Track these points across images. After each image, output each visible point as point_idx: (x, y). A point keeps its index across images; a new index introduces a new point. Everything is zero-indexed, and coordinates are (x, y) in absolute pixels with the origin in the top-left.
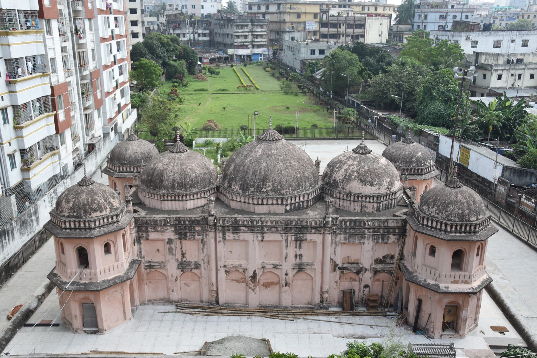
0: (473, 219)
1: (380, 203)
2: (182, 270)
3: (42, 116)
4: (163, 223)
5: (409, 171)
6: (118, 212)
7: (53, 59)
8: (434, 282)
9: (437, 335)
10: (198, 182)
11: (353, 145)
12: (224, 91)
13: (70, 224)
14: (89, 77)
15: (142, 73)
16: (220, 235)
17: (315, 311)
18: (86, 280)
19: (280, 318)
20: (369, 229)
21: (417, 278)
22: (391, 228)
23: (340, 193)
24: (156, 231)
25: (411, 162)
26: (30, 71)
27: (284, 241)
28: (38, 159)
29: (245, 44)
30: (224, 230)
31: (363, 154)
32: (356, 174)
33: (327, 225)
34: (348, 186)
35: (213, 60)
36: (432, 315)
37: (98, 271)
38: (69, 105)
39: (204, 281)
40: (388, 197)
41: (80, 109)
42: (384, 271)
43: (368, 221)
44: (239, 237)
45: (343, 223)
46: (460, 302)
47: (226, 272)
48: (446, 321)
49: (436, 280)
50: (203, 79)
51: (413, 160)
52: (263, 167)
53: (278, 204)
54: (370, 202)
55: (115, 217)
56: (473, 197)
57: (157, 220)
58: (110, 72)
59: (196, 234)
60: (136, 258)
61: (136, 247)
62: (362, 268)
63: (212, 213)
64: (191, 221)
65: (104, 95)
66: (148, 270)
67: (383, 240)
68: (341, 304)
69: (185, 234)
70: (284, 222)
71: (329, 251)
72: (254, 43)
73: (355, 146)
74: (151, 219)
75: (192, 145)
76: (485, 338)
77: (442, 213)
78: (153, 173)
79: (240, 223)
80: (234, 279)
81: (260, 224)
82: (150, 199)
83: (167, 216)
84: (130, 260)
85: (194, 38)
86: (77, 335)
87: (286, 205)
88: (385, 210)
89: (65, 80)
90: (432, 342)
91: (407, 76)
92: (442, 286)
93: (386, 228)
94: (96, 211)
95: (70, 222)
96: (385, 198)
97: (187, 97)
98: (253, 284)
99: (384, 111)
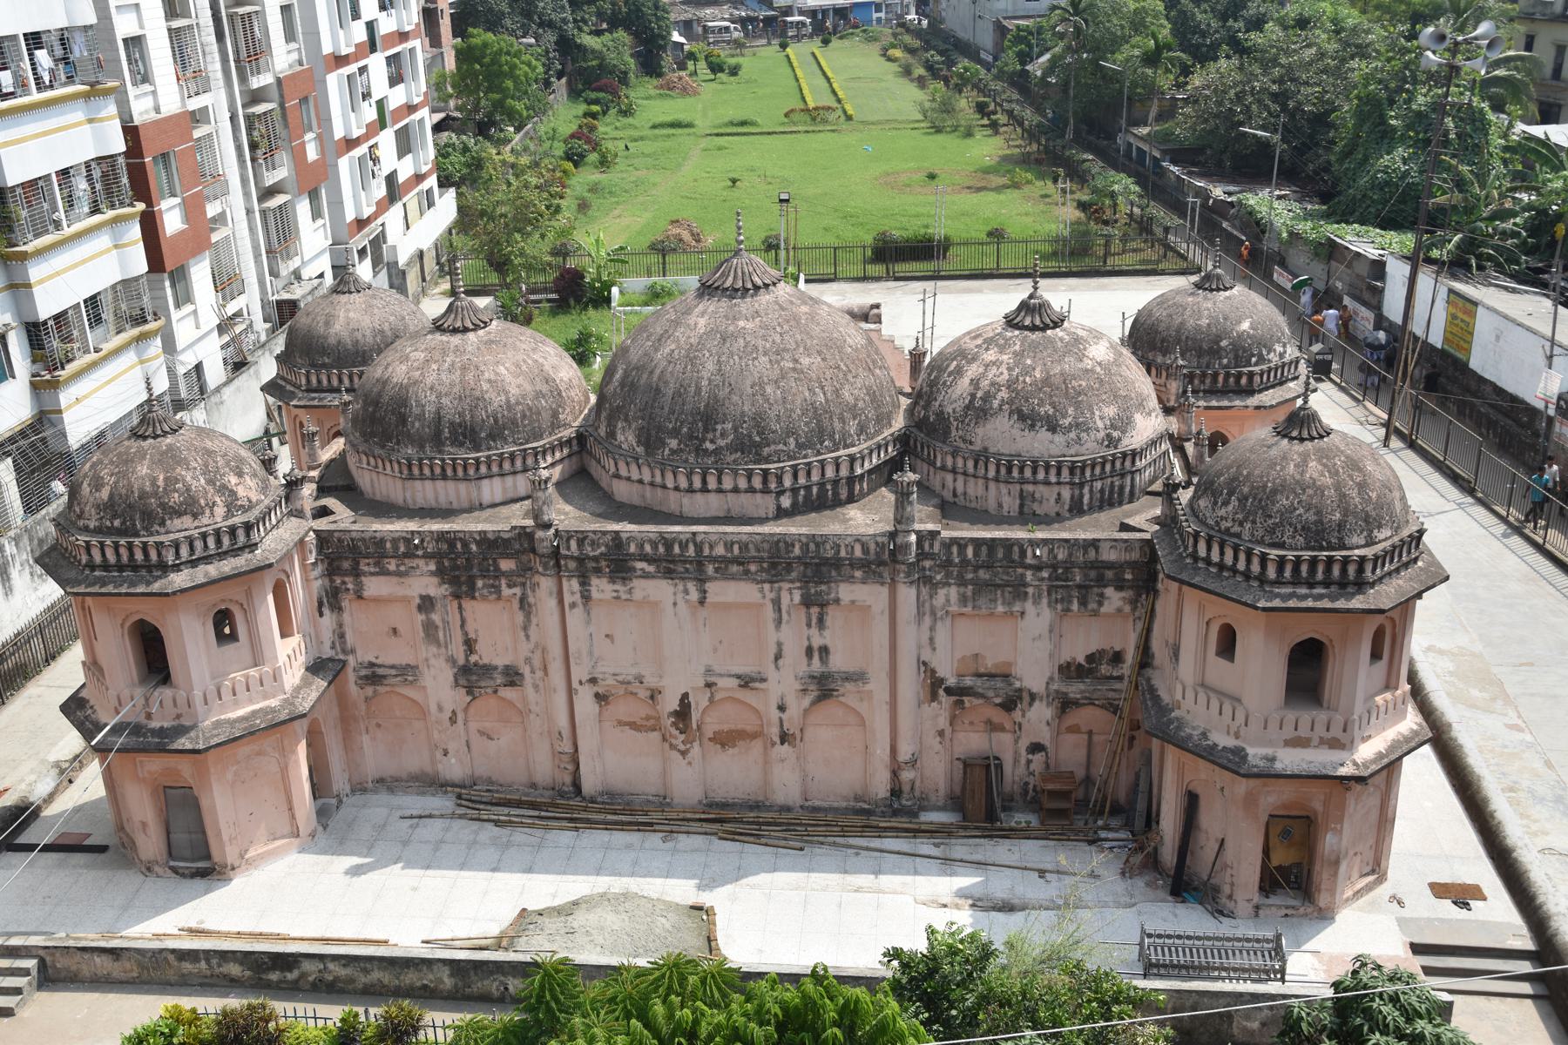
1: (1081, 485)
4: (402, 549)
5: (1208, 381)
6: (251, 517)
7: (135, 43)
8: (1230, 742)
9: (1243, 908)
10: (514, 422)
12: (742, 126)
13: (103, 554)
14: (275, 94)
15: (475, 74)
16: (572, 586)
17: (874, 820)
19: (763, 840)
20: (1038, 568)
21: (1179, 728)
22: (1110, 566)
23: (954, 455)
24: (384, 572)
25: (1215, 352)
27: (770, 606)
28: (87, 351)
30: (585, 570)
31: (1034, 328)
32: (1004, 394)
33: (900, 558)
34: (980, 431)
36: (1229, 845)
37: (198, 694)
40: (1108, 467)
41: (247, 194)
43: (1034, 543)
44: (630, 591)
45: (955, 549)
46: (1318, 806)
47: (599, 697)
49: (1237, 736)
50: (684, 89)
51: (1224, 343)
52: (705, 374)
53: (751, 490)
54: (1047, 483)
55: (241, 533)
56: (1360, 470)
57: (382, 541)
59: (503, 582)
60: (328, 653)
62: (1020, 690)
63: (546, 518)
66: (369, 690)
67: (1083, 603)
68: (956, 802)
70: (766, 546)
71: (910, 638)
74: (367, 536)
75: (608, 300)
76: (1402, 922)
77: (1254, 522)
78: (380, 394)
79: (633, 548)
81: (691, 551)
82: (374, 475)
83: (412, 526)
87: (780, 493)
89: (184, 105)
90: (1225, 928)
92: (1255, 753)
94: (180, 514)
96: (1098, 470)
98: (682, 737)
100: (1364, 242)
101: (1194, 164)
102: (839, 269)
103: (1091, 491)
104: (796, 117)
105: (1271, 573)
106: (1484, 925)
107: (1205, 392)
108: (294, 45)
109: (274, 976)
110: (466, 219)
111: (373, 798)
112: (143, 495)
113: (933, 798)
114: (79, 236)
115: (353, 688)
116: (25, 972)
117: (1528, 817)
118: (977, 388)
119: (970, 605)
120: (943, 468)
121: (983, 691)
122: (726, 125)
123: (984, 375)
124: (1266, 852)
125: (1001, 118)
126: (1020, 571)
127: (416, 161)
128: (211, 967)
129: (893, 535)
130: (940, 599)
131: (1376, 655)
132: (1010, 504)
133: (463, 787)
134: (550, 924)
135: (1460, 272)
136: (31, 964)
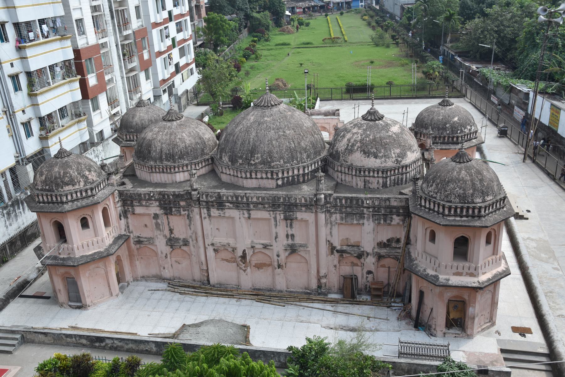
0: (478, 200)
1: (386, 178)
2: (172, 246)
3: (64, 81)
5: (442, 139)
6: (93, 186)
9: (439, 333)
10: (188, 153)
12: (307, 45)
13: (43, 198)
14: (132, 37)
16: (204, 211)
18: (64, 254)
20: (368, 208)
21: (416, 267)
22: (394, 207)
24: (141, 205)
25: (445, 129)
26: (46, 35)
27: (273, 220)
28: (59, 127)
30: (208, 206)
31: (371, 120)
32: (359, 144)
33: (318, 203)
34: (350, 158)
36: (434, 310)
37: (75, 246)
38: (103, 68)
39: (194, 259)
40: (396, 171)
41: (121, 72)
42: (389, 257)
43: (366, 199)
44: (224, 213)
46: (466, 297)
48: (451, 317)
50: (289, 31)
51: (448, 125)
52: (252, 137)
54: (374, 177)
56: (481, 174)
57: (141, 194)
58: (161, 30)
59: (182, 209)
60: (123, 233)
61: (123, 221)
62: (363, 251)
63: (195, 187)
64: (174, 195)
65: (153, 56)
66: (138, 246)
67: (385, 221)
69: (171, 208)
70: (271, 198)
71: (324, 232)
74: (135, 192)
76: (498, 341)
77: (441, 193)
78: (142, 143)
79: (225, 198)
80: (224, 258)
81: (245, 200)
83: (151, 189)
84: (116, 235)
86: (63, 309)
87: (277, 179)
88: (394, 186)
91: (510, 20)
92: (442, 278)
93: (388, 208)
94: (68, 185)
96: (392, 172)
97: (265, 53)
98: (244, 265)
99: (481, 63)
100: (523, 86)
101: (468, 57)
103: (390, 180)
104: (326, 41)
105: (447, 212)
106: (529, 343)
107: (441, 143)
108: (140, 20)
109: (97, 344)
110: (205, 79)
112: (56, 178)
113: (333, 289)
115: (133, 246)
116: (17, 339)
117: (555, 303)
119: (344, 221)
120: (337, 171)
121: (349, 252)
123: (352, 137)
124: (448, 313)
125: (400, 41)
126: (362, 208)
127: (187, 59)
128: (76, 340)
129: (316, 195)
131: (488, 242)
132: (361, 184)
133: (170, 280)
134: (191, 330)
135: (558, 97)
136: (18, 336)
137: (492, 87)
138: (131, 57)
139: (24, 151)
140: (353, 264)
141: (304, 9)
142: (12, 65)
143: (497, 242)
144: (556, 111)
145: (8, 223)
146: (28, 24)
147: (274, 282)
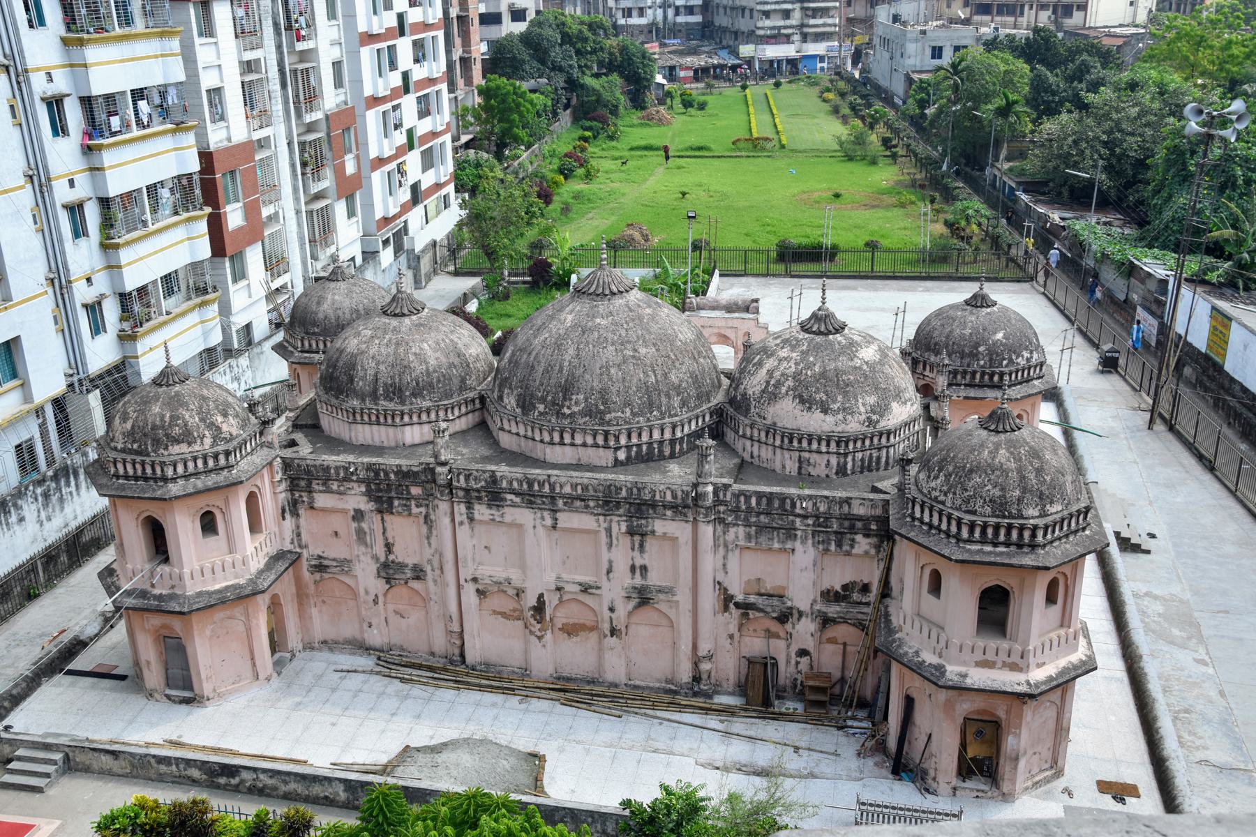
0: (1032, 512)
1: (846, 455)
2: (388, 580)
3: (177, 218)
4: (342, 475)
5: (968, 377)
6: (230, 446)
9: (944, 788)
10: (431, 385)
11: (964, 292)
12: (699, 151)
14: (323, 126)
16: (461, 509)
17: (678, 699)
18: (163, 588)
20: (805, 517)
21: (899, 646)
22: (859, 518)
25: (974, 355)
26: (145, 120)
27: (603, 534)
28: (160, 314)
29: (783, 31)
30: (470, 498)
31: (819, 333)
32: (790, 383)
33: (700, 503)
34: (771, 410)
35: (700, 74)
37: (186, 571)
38: (258, 191)
39: (434, 608)
40: (867, 442)
41: (297, 199)
43: (801, 498)
44: (502, 515)
46: (1001, 714)
48: (970, 754)
51: (981, 349)
52: (567, 357)
53: (596, 445)
54: (819, 452)
56: (1039, 458)
57: (328, 468)
58: (384, 113)
59: (413, 503)
61: (289, 522)
62: (791, 608)
63: (443, 458)
64: (400, 472)
65: (366, 167)
66: (317, 576)
67: (839, 545)
68: (742, 689)
69: (390, 500)
70: (601, 488)
71: (709, 563)
72: (806, 30)
73: (968, 296)
74: (318, 463)
75: (568, 284)
77: (955, 493)
78: (337, 360)
79: (504, 484)
81: (547, 489)
83: (351, 458)
84: (272, 550)
85: (665, 17)
86: (152, 702)
87: (617, 449)
88: (861, 472)
92: (952, 671)
94: (177, 441)
95: (124, 462)
96: (859, 444)
97: (607, 165)
98: (539, 626)
99: (1072, 209)
100: (1157, 265)
101: (1043, 194)
102: (749, 266)
103: (854, 460)
105: (965, 534)
107: (966, 385)
108: (341, 90)
109: (222, 780)
110: (475, 219)
111: (317, 654)
112: (154, 427)
114: (160, 231)
115: (306, 575)
116: (55, 763)
117: (1195, 734)
118: (771, 377)
119: (753, 541)
120: (744, 436)
121: (759, 608)
122: (687, 150)
123: (777, 367)
124: (963, 746)
125: (901, 151)
126: (791, 518)
127: (438, 173)
128: (179, 770)
129: (695, 486)
130: (731, 535)
131: (1051, 599)
132: (791, 467)
133: (382, 651)
134: (422, 759)
135: (1228, 292)
136: (58, 756)
137: (1091, 263)
138: (318, 168)
139: (84, 364)
140: (770, 635)
141: (696, 71)
142: (72, 183)
143: (1069, 600)
144: (1221, 322)
145: (43, 514)
146: (110, 98)
147: (600, 664)
